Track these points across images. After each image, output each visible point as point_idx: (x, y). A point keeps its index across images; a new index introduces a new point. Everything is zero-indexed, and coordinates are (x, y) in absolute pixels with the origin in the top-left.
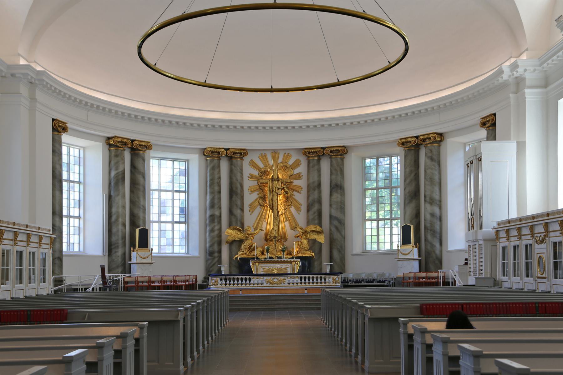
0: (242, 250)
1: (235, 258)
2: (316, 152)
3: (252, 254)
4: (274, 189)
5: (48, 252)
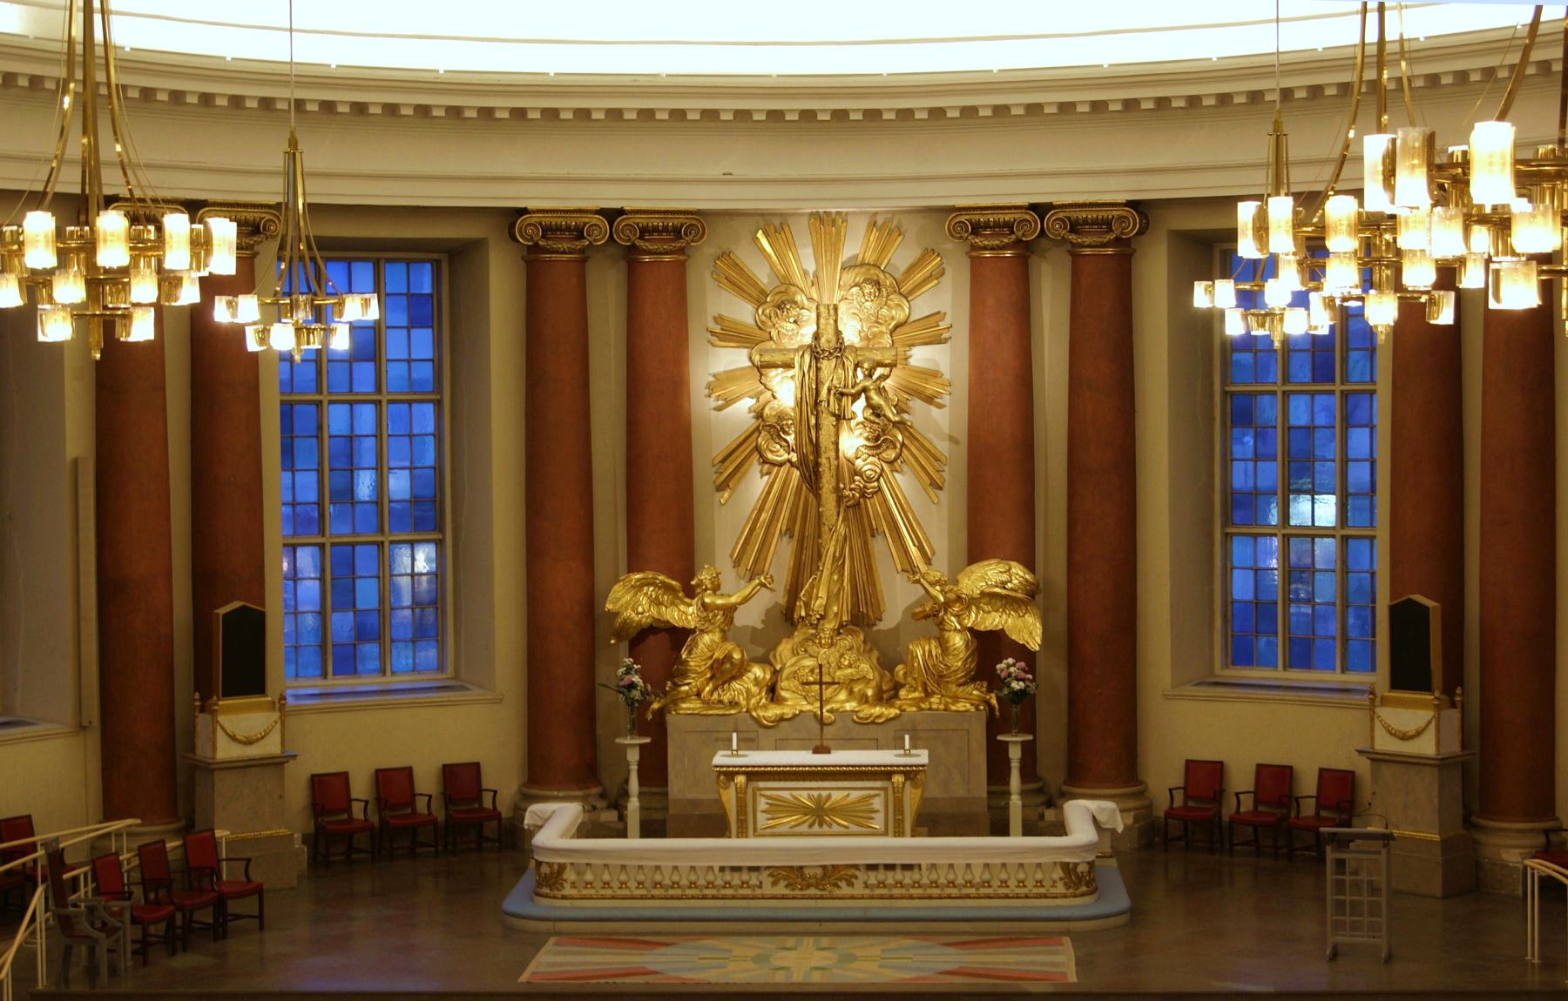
2: (1009, 226)
3: (726, 698)
4: (824, 392)
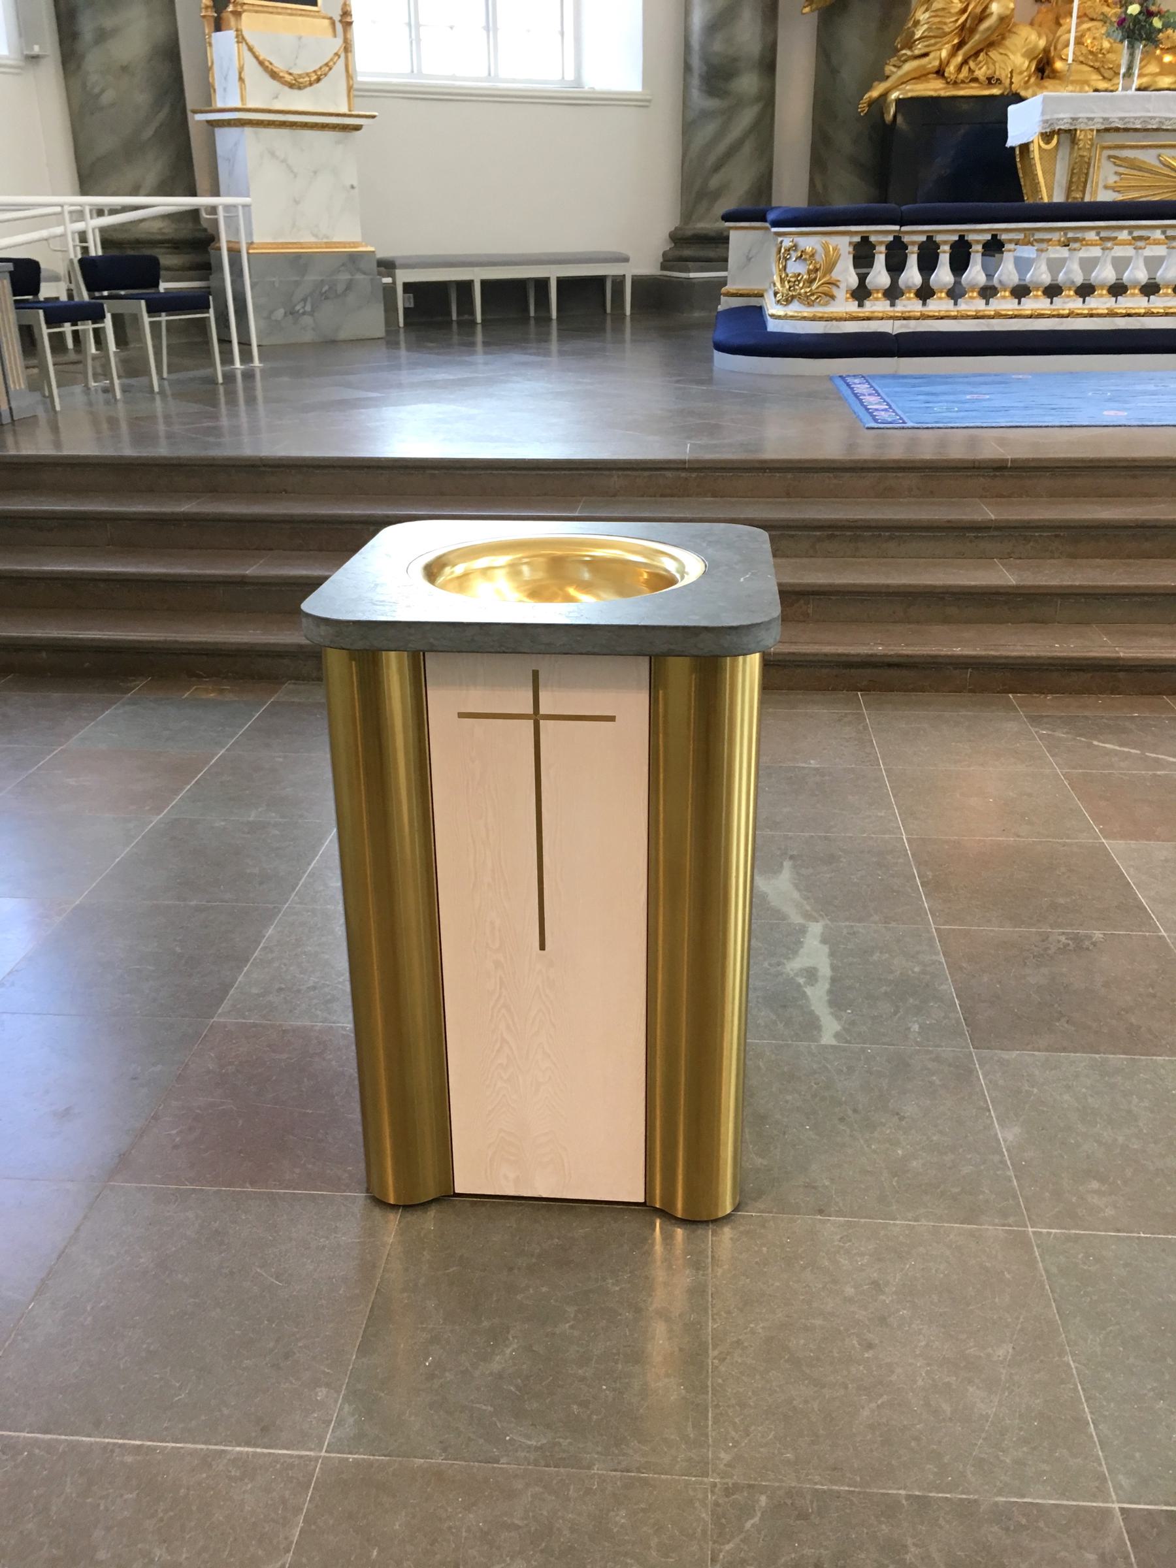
0: (919, 48)
1: (871, 103)
3: (981, 73)
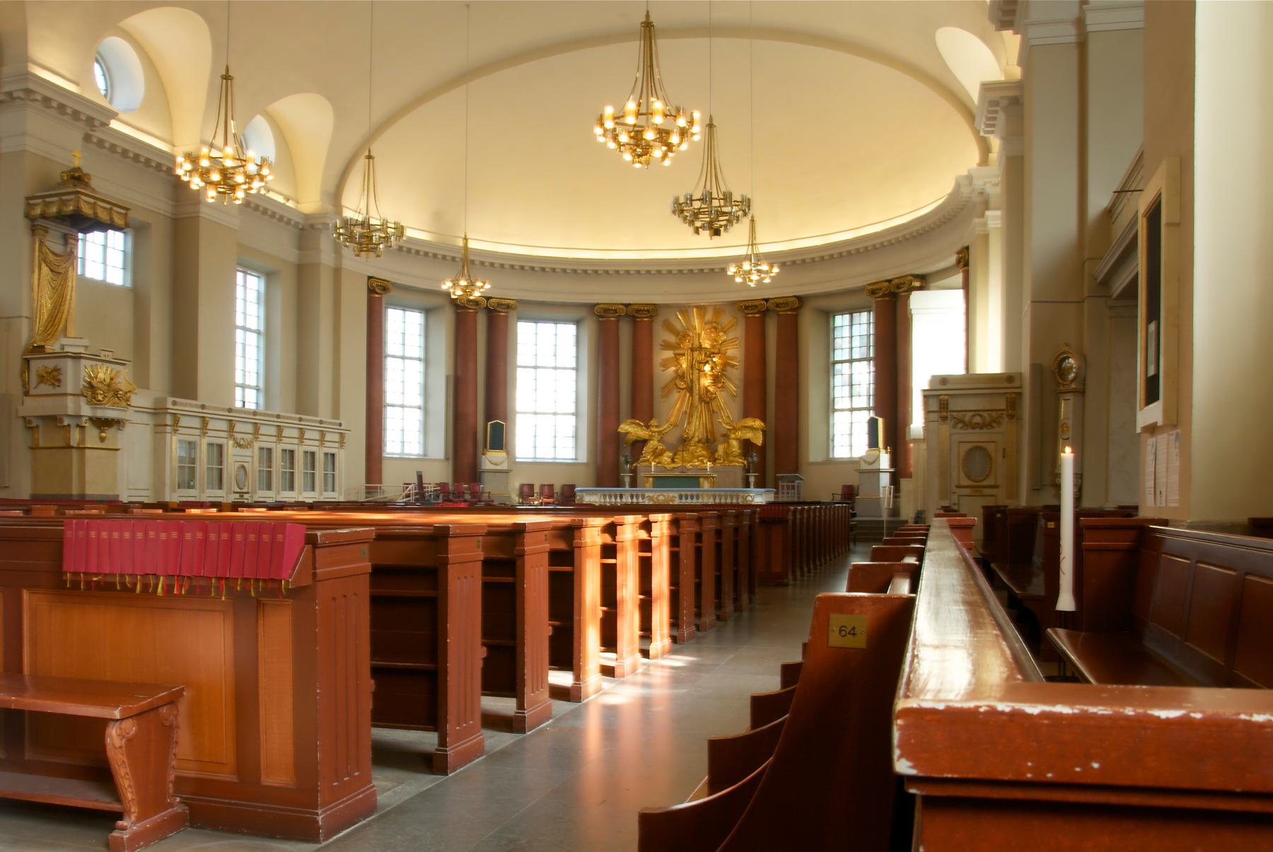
5: (297, 449)
